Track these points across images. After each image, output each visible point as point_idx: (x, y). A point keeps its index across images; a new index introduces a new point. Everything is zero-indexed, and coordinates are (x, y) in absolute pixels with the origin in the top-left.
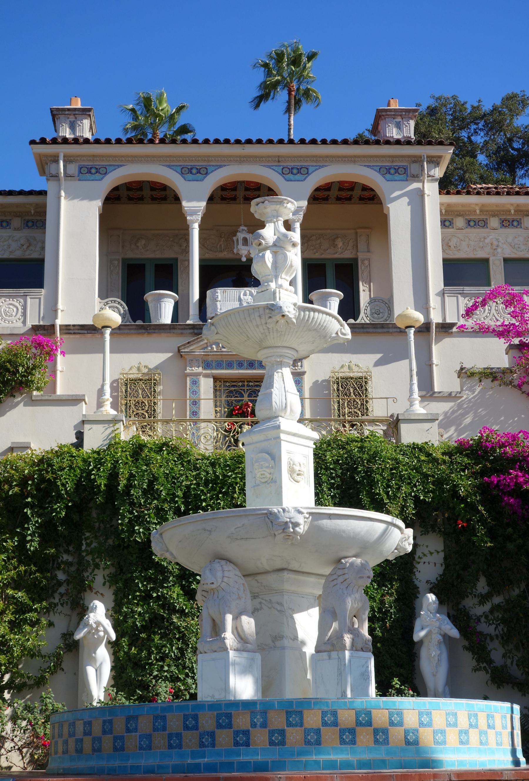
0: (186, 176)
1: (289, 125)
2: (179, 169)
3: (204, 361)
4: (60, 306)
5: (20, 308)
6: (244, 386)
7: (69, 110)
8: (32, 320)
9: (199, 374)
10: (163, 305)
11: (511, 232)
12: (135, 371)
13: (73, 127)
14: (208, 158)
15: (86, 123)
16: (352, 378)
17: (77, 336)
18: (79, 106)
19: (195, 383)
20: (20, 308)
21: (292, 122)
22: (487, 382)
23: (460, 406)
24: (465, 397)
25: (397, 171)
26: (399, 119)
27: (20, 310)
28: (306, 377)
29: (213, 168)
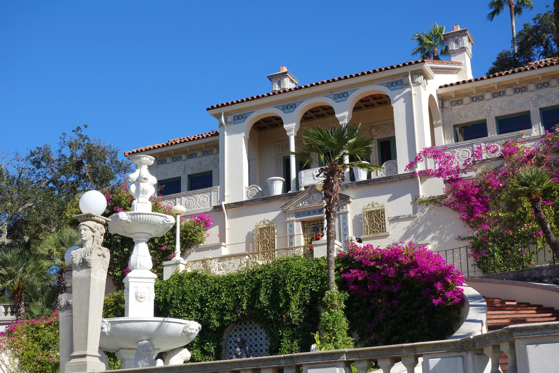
0: (336, 100)
1: (512, 27)
2: (333, 97)
3: (295, 213)
4: (226, 194)
5: (470, 152)
6: (318, 224)
7: (276, 75)
8: (214, 204)
9: (293, 221)
10: (274, 185)
11: (499, 100)
12: (262, 223)
13: (279, 84)
14: (295, 98)
15: (465, 39)
16: (374, 211)
17: (233, 209)
18: (459, 29)
19: (292, 226)
20: (470, 152)
21: (514, 25)
22: (431, 205)
23: (416, 222)
24: (418, 216)
25: (397, 84)
26: (456, 38)
27: (209, 199)
28: (349, 215)
29: (298, 103)
